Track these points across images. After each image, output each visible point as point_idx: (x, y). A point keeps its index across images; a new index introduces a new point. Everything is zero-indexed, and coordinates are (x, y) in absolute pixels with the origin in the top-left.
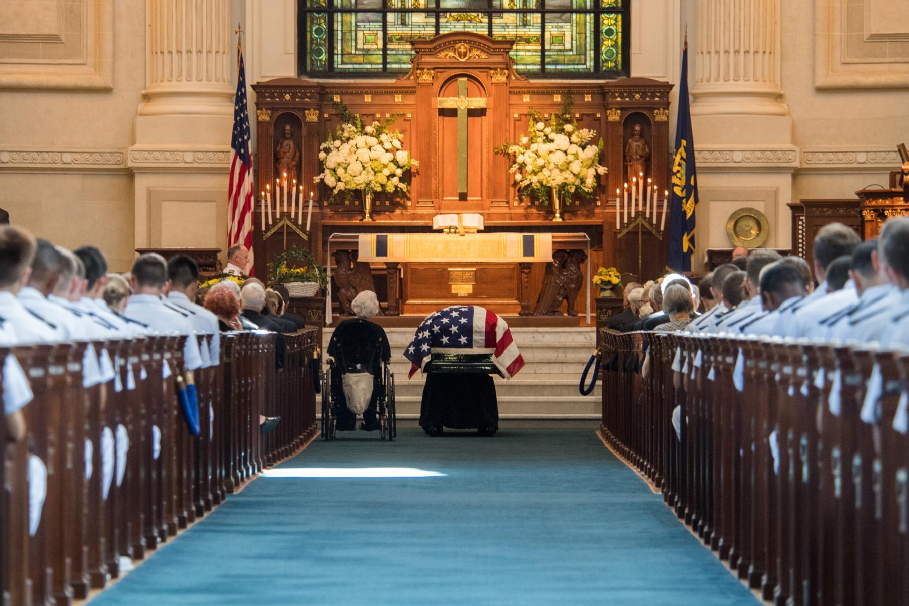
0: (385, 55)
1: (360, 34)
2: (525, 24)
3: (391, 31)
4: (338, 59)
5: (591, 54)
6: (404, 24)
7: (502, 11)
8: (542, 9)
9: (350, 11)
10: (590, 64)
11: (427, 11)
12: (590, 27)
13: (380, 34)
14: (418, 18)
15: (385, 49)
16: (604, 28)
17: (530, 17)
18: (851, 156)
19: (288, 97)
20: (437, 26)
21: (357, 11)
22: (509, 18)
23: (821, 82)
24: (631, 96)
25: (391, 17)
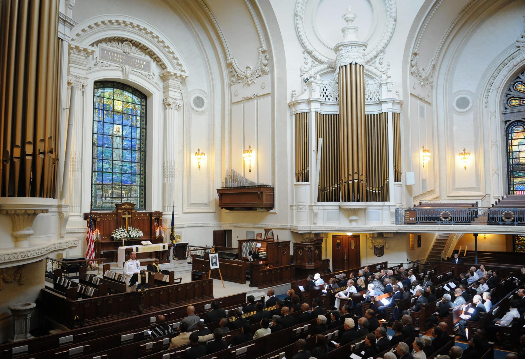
0: (102, 206)
1: (97, 202)
2: (128, 200)
3: (103, 201)
4: (93, 207)
5: (139, 206)
6: (106, 200)
7: (124, 198)
8: (131, 197)
9: (95, 197)
10: (139, 208)
11: (110, 197)
12: (139, 201)
13: (101, 202)
14: (108, 199)
15: (102, 205)
16: (141, 201)
17: (129, 199)
18: (189, 225)
19: (94, 216)
20: (112, 200)
21: (97, 197)
22: (125, 199)
23: (184, 212)
24: (156, 215)
25: (103, 198)
